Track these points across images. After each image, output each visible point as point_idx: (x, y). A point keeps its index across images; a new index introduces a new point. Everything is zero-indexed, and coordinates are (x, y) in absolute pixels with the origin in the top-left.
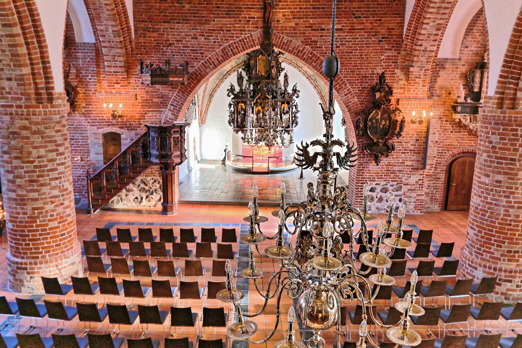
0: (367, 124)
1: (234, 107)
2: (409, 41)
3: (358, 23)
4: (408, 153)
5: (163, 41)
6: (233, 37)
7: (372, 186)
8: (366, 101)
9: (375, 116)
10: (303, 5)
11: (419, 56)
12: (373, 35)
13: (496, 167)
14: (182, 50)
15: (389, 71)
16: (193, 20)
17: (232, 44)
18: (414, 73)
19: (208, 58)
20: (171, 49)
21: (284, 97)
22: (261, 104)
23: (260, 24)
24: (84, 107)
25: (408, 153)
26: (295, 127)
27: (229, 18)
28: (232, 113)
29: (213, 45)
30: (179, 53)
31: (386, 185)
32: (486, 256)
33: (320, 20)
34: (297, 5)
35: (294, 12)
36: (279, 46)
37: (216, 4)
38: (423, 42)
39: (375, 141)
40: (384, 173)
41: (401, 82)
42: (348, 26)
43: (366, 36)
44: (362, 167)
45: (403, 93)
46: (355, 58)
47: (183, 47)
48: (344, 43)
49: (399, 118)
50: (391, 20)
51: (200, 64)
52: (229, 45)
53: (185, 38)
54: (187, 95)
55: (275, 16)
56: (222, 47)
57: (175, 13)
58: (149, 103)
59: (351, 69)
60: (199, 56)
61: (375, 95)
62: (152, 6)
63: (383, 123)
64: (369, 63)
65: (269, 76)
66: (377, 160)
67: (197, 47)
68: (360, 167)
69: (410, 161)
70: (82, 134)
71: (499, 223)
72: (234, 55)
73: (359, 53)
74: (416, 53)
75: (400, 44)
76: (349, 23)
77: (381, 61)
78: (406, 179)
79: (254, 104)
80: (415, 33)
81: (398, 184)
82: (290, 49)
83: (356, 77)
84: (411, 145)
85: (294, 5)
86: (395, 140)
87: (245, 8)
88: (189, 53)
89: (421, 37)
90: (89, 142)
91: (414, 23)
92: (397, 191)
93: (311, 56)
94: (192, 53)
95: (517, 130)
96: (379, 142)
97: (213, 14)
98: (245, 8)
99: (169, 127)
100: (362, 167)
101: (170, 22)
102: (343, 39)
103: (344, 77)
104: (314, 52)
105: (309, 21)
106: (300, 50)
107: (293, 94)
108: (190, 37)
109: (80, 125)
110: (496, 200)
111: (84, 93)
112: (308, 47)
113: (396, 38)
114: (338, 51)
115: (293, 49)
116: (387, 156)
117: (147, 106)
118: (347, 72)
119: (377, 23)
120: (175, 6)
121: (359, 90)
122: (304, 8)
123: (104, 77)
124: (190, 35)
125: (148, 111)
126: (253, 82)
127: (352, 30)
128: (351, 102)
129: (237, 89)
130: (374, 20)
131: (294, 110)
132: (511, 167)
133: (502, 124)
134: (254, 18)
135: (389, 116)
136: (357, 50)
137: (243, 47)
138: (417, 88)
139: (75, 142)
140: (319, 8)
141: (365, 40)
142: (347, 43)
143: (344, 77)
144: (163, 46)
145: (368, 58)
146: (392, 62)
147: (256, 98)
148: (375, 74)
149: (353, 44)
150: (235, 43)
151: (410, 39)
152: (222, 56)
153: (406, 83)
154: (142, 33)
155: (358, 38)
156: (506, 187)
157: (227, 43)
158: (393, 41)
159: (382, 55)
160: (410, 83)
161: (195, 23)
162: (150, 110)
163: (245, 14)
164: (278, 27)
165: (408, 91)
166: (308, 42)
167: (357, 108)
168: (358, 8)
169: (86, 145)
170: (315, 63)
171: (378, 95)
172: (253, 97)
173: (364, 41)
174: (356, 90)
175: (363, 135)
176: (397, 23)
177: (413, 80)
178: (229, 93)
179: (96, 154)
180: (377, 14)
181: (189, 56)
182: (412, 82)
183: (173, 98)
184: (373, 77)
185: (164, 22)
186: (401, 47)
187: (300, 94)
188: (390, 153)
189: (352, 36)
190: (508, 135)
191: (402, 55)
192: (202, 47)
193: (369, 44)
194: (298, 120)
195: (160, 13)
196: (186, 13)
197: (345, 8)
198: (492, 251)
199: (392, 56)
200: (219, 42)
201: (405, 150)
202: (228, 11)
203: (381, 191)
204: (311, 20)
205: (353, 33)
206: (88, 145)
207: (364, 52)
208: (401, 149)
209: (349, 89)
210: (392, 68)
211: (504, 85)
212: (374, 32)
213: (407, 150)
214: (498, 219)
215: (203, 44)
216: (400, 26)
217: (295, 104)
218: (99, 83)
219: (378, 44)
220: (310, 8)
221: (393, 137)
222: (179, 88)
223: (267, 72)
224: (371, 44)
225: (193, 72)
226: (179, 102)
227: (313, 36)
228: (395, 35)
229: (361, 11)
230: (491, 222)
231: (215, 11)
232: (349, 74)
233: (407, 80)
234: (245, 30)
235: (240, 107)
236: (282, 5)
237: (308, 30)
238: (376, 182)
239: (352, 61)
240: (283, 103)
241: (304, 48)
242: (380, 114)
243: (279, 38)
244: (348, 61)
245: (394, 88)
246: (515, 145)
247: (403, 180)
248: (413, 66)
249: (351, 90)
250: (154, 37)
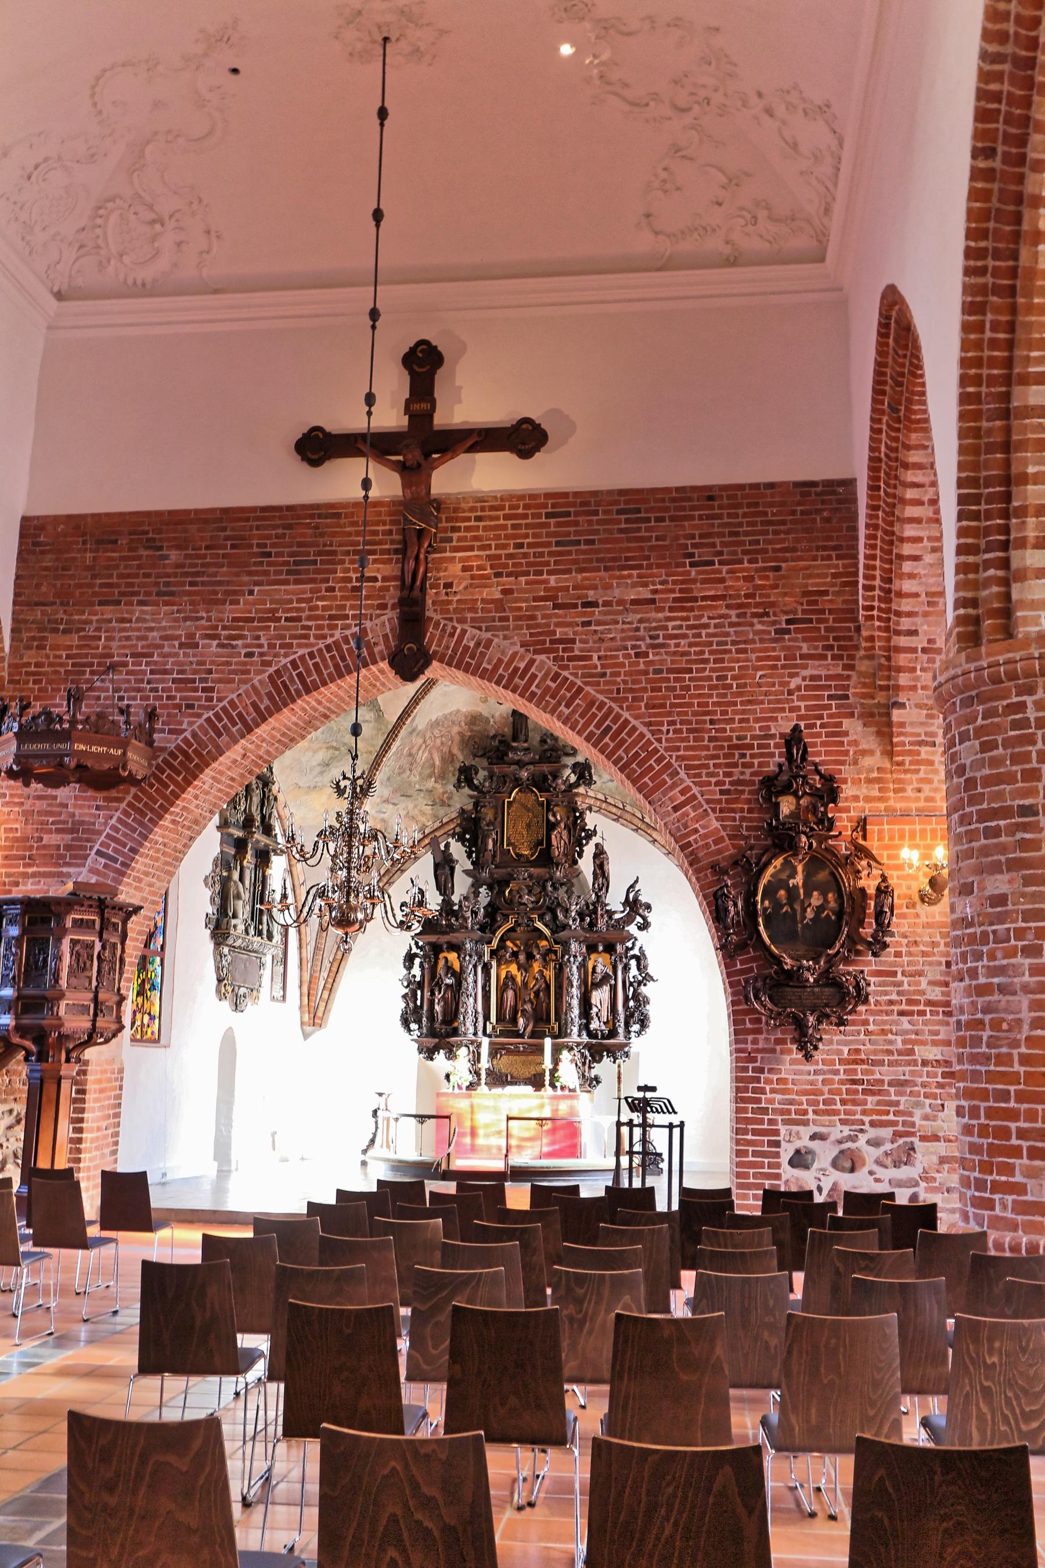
0: (755, 904)
1: (421, 965)
2: (877, 623)
3: (704, 581)
4: (922, 1013)
5: (94, 656)
6: (306, 637)
7: (798, 1144)
8: (748, 829)
9: (784, 876)
10: (527, 536)
11: (914, 670)
12: (755, 615)
13: (984, 851)
14: (149, 683)
15: (822, 726)
16: (189, 593)
17: (302, 658)
18: (908, 729)
19: (225, 703)
20: (112, 681)
21: (592, 924)
22: (515, 954)
23: (392, 596)
25: (922, 1013)
26: (639, 1034)
27: (297, 582)
28: (414, 987)
29: (245, 664)
30: (139, 690)
31: (853, 1139)
32: (1004, 1207)
33: (579, 577)
34: (507, 537)
35: (499, 557)
36: (452, 657)
37: (259, 545)
38: (918, 620)
39: (788, 963)
40: (838, 1092)
41: (867, 762)
42: (673, 591)
43: (734, 619)
44: (754, 1070)
45: (880, 799)
46: (702, 687)
47: (152, 672)
48: (661, 641)
49: (870, 885)
50: (815, 567)
51: (201, 721)
52: (293, 663)
53: (162, 647)
54: (151, 820)
55: (438, 570)
56: (271, 670)
57: (136, 576)
58: (31, 848)
59: (690, 722)
60: (199, 699)
61: (777, 805)
62: (74, 559)
63: (816, 900)
64: (750, 702)
65: (546, 859)
66: (806, 1045)
67: (195, 672)
68: (746, 1069)
69: (935, 1043)
71: (1025, 1060)
72: (308, 691)
73: (712, 670)
74: (902, 659)
75: (851, 639)
76: (674, 582)
77: (790, 693)
78: (926, 1118)
79: (493, 953)
80: (887, 596)
81: (897, 1135)
82: (484, 665)
83: (707, 748)
84: (931, 983)
85: (497, 537)
86: (869, 963)
87: (348, 553)
88: (170, 689)
89: (906, 605)
91: (878, 563)
92: (896, 1165)
93: (553, 685)
94: (177, 690)
95: (1022, 707)
96: (801, 967)
97: (250, 573)
98: (348, 553)
99: (58, 901)
100: (754, 1070)
101: (118, 603)
102: (656, 629)
103: (667, 749)
104: (565, 673)
105: (546, 582)
106: (516, 669)
107: (629, 920)
108: (176, 643)
110: (1001, 971)
112: (543, 657)
113: (835, 620)
114: (642, 667)
115: (496, 668)
116: (841, 1022)
117: (23, 858)
118: (675, 731)
119: (767, 578)
120: (139, 558)
121: (722, 792)
122: (530, 546)
124: (178, 637)
125: (25, 875)
126: (485, 875)
127: (685, 601)
128: (696, 831)
129: (434, 901)
130: (757, 570)
131: (634, 971)
132: (1027, 836)
133: (982, 699)
134: (375, 579)
135: (835, 879)
136: (706, 661)
137: (337, 667)
138: (929, 781)
140: (578, 542)
141: (732, 630)
142: (672, 642)
143: (667, 749)
144: (92, 673)
145: (745, 685)
146: (830, 697)
147: (499, 934)
148: (772, 737)
149: (690, 645)
150: (312, 655)
151: (880, 619)
152: (269, 695)
153: (887, 765)
154: (34, 638)
155: (706, 626)
156: (1024, 912)
157: (286, 656)
158: (827, 629)
159: (792, 675)
160: (901, 764)
161: (192, 603)
162: (30, 870)
163: (347, 570)
164: (449, 602)
165: (896, 791)
166: (544, 642)
167: (719, 852)
168: (701, 536)
170: (567, 706)
171: (786, 806)
172: (488, 927)
173: (727, 634)
174: (713, 793)
175: (742, 947)
176: (834, 576)
177: (910, 753)
180: (765, 551)
181: (169, 698)
182: (908, 759)
183: (108, 830)
184: (768, 746)
185: (101, 604)
186: (857, 648)
188: (853, 1011)
189: (683, 619)
190: (998, 729)
191: (861, 674)
192: (210, 672)
193: (745, 642)
194: (651, 1010)
195: (94, 577)
196: (168, 575)
197: (657, 539)
198: (1018, 1178)
199: (828, 678)
200: (261, 654)
201: (910, 1002)
202: (296, 563)
203: (835, 1164)
204: (552, 578)
205: (692, 609)
207: (733, 669)
208: (894, 997)
209: (688, 789)
210: (830, 716)
211: (971, 576)
212: (757, 605)
213: (917, 1002)
214: (1016, 1044)
215: (212, 663)
216: (845, 584)
217: (636, 951)
219: (775, 640)
220: (549, 544)
221: (858, 953)
222: (129, 798)
223: (540, 843)
224: (753, 642)
225: (178, 747)
226: (124, 845)
227: (557, 625)
228: (831, 611)
229: (714, 545)
230: (1001, 1060)
231: (255, 564)
232: (683, 740)
233: (890, 754)
234: (346, 617)
235: (441, 963)
236: (460, 539)
237: (544, 608)
238: (813, 1129)
239: (691, 696)
240: (592, 949)
241: (532, 662)
242: (800, 868)
243: (452, 635)
244: (676, 697)
245: (845, 781)
246: (1026, 757)
247: (917, 1119)
248: (902, 706)
249: (695, 790)
250: (70, 647)
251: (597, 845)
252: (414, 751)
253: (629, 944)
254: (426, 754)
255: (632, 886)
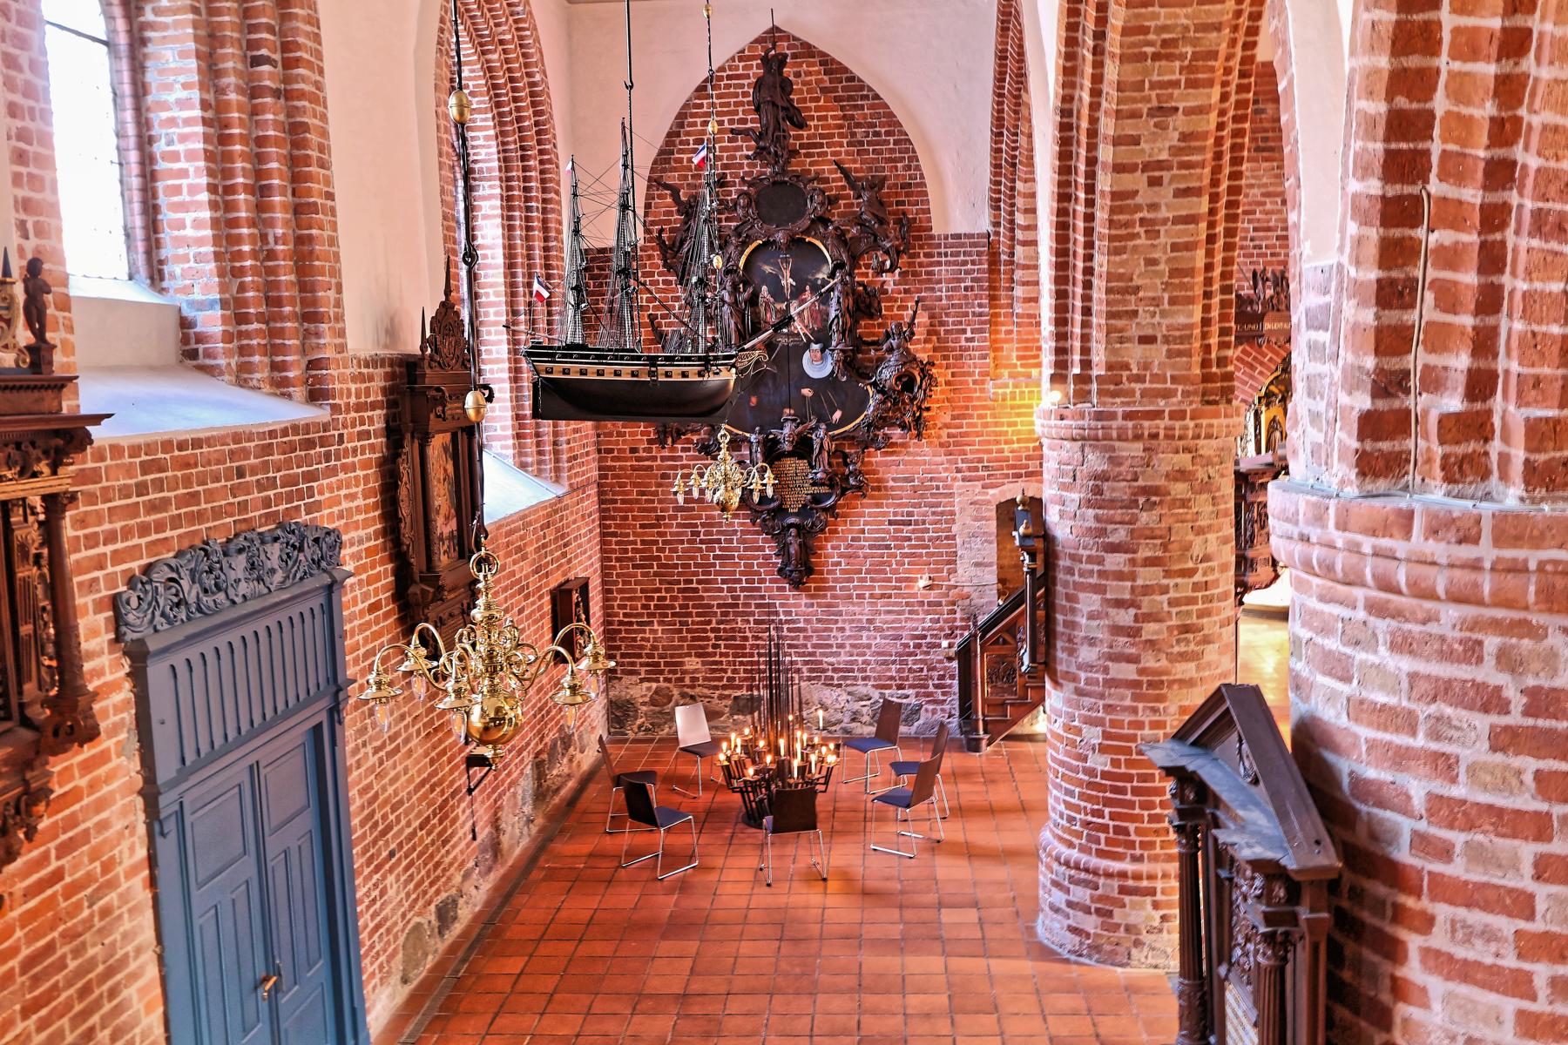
24: (947, 426)
47: (1255, 229)
53: (1264, 204)
70: (938, 505)
88: (1274, 246)
90: (955, 529)
109: (931, 479)
111: (948, 383)
123: (1009, 332)
139: (913, 531)
169: (947, 538)
179: (977, 565)
181: (1272, 255)
196: (1266, 130)
206: (953, 538)
218: (996, 350)
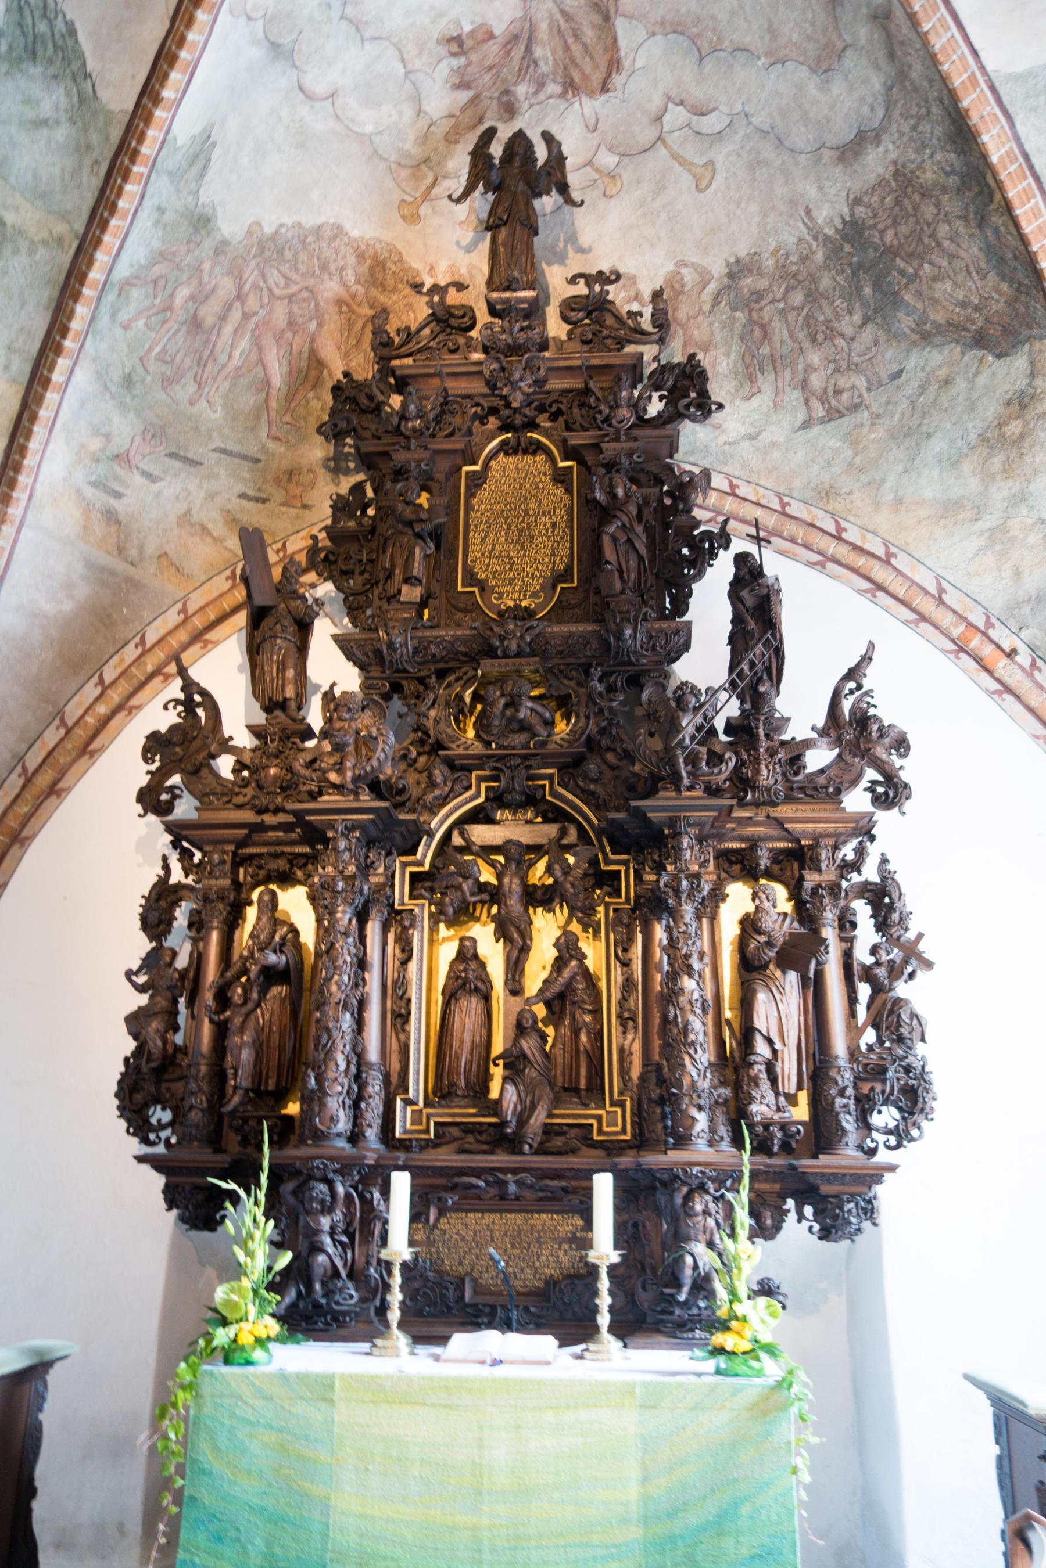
1: (197, 925)
26: (901, 1136)
131: (866, 934)
178: (158, 777)
187: (909, 770)
217: (870, 873)
251: (742, 560)
252: (209, 312)
253: (848, 851)
254: (244, 344)
255: (853, 674)
